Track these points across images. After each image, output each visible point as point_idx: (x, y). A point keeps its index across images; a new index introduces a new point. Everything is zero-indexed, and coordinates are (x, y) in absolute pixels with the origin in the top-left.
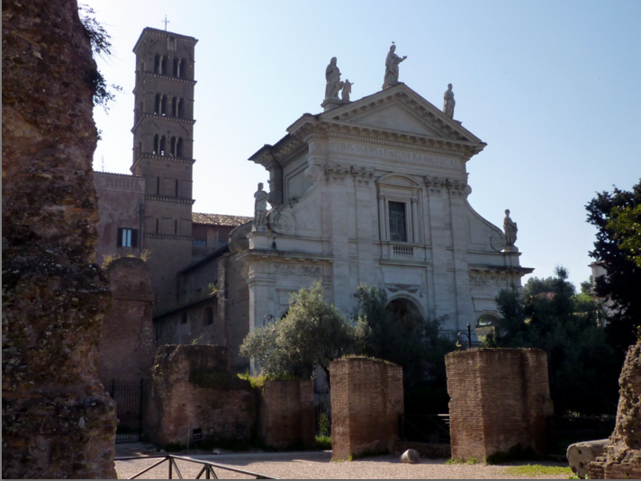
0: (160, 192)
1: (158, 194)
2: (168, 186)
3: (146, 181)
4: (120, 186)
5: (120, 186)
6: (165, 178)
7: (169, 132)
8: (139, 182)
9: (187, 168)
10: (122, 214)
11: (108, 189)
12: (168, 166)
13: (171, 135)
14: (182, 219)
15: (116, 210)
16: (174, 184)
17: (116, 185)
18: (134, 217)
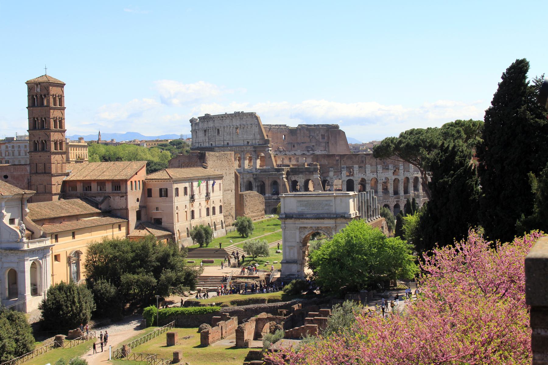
0: (38, 171)
1: (37, 172)
2: (41, 167)
3: (30, 167)
4: (19, 171)
5: (19, 171)
6: (39, 163)
7: (40, 138)
8: (27, 168)
9: (49, 156)
10: (21, 185)
11: (14, 173)
12: (40, 156)
13: (41, 139)
14: (47, 184)
15: (18, 184)
16: (44, 166)
17: (18, 171)
18: (26, 186)
